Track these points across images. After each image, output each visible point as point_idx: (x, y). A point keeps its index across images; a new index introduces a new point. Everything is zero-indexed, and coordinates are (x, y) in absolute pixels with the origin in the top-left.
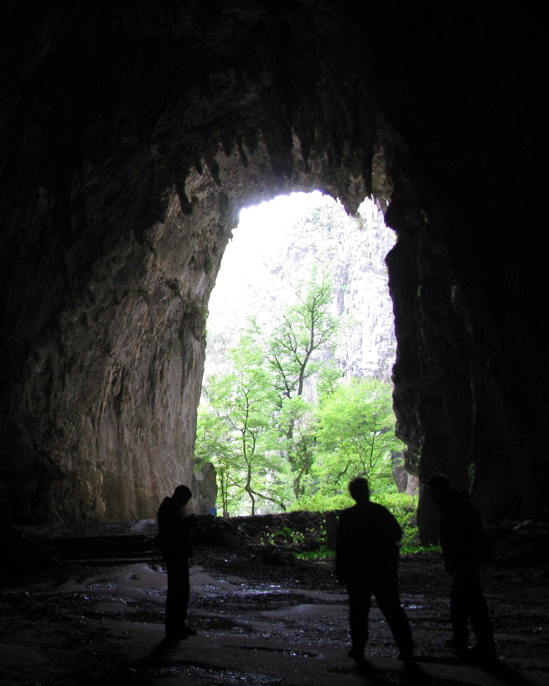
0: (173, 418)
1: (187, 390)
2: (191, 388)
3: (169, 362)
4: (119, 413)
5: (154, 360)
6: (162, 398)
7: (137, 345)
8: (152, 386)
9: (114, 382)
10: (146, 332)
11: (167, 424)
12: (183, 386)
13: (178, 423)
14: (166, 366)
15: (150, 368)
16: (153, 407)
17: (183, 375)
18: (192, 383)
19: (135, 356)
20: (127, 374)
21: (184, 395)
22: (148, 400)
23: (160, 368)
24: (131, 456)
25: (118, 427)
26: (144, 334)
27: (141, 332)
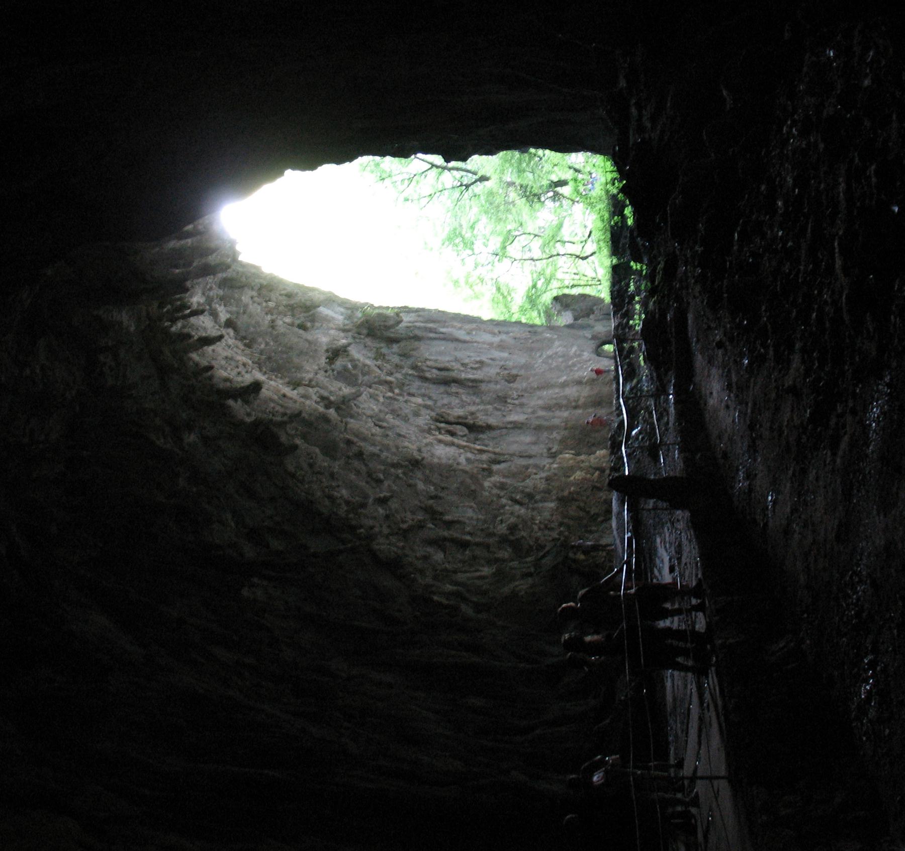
0: (497, 354)
1: (461, 334)
2: (460, 328)
3: (426, 359)
4: (489, 427)
5: (425, 379)
6: (472, 368)
7: (406, 402)
9: (452, 434)
13: (501, 347)
15: (434, 383)
16: (481, 381)
17: (444, 339)
18: (453, 327)
19: (420, 405)
21: (467, 338)
22: (473, 387)
23: (434, 371)
24: (541, 413)
25: (506, 428)
27: (390, 398)
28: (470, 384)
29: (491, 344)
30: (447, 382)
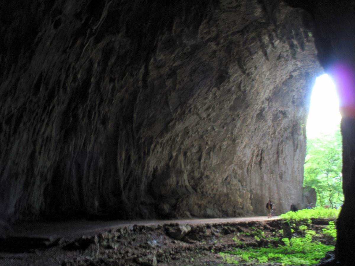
0: (290, 170)
1: (296, 157)
2: (299, 157)
4: (261, 168)
5: (278, 145)
6: (283, 161)
8: (278, 157)
9: (257, 156)
10: (272, 134)
12: (294, 155)
19: (268, 144)
20: (264, 152)
21: (295, 159)
25: (261, 174)
29: (293, 168)
30: (278, 153)
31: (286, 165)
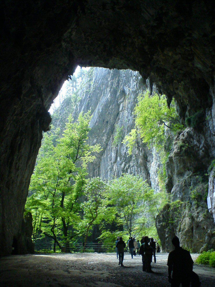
0: (19, 179)
1: (30, 163)
6: (17, 163)
11: (15, 182)
13: (21, 182)
14: (24, 141)
21: (28, 165)
23: (19, 142)
26: (15, 115)
28: (10, 161)
31: (18, 170)
